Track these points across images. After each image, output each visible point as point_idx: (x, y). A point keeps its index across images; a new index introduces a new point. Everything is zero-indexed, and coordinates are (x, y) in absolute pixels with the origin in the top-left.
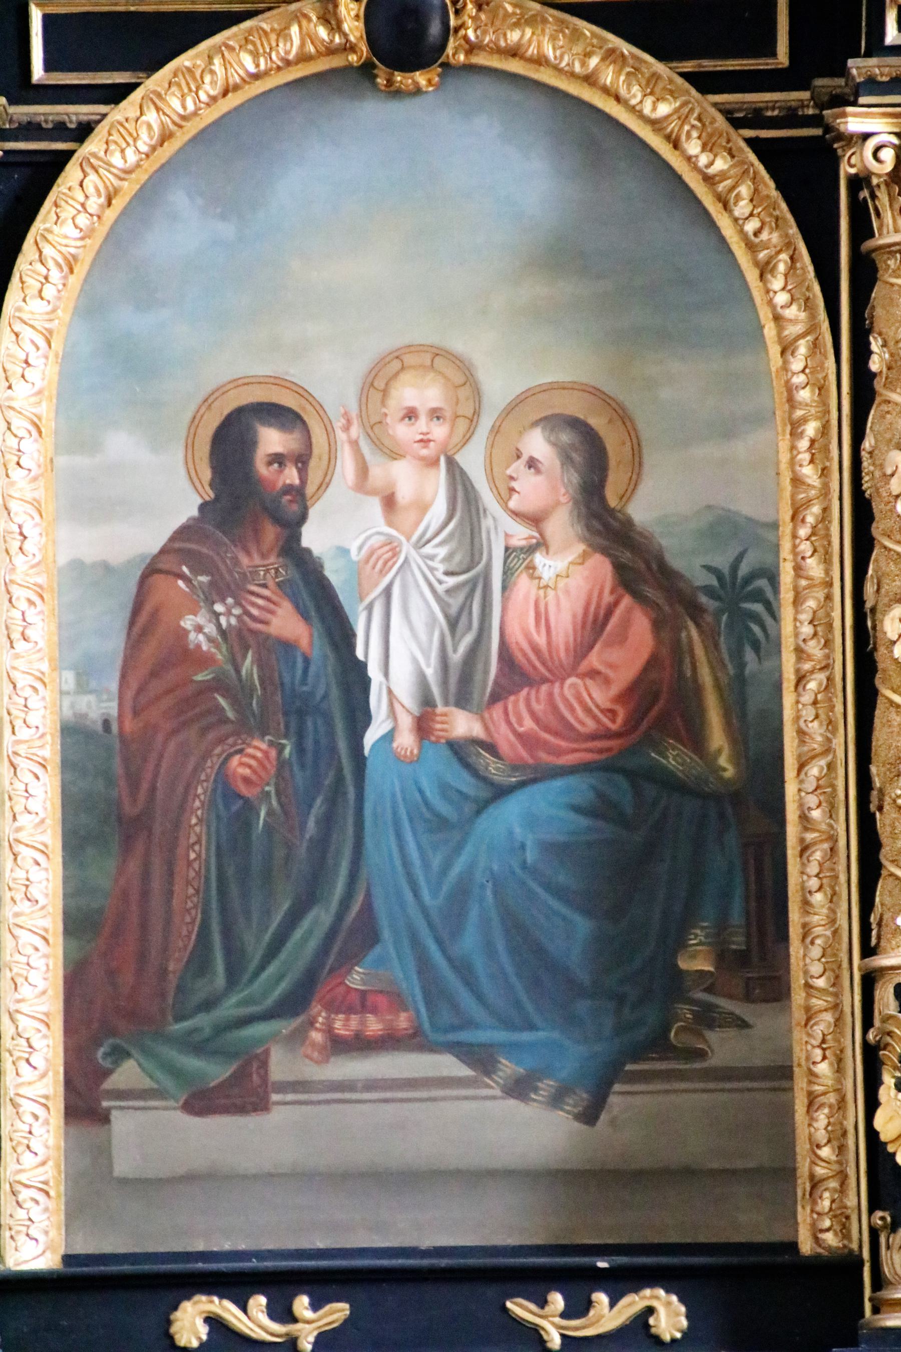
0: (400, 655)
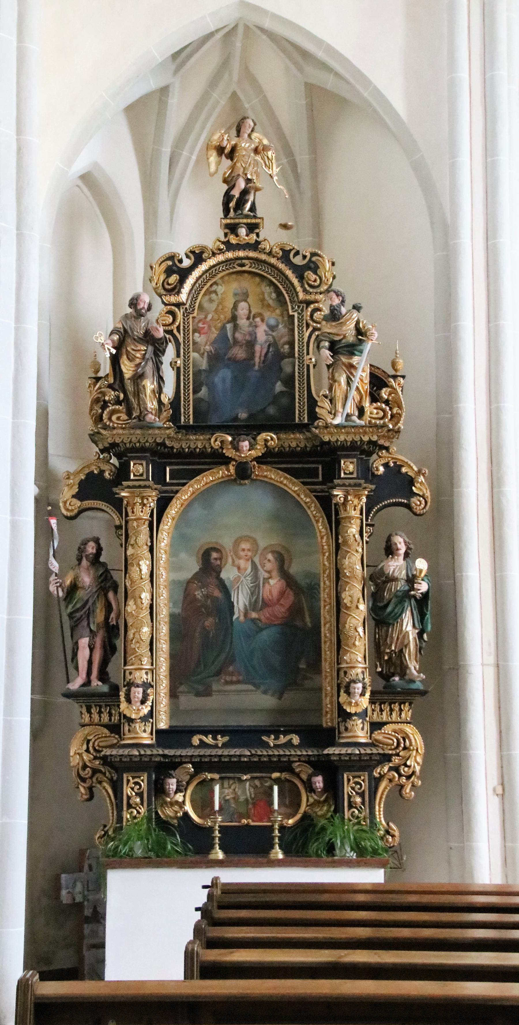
0: (241, 600)
